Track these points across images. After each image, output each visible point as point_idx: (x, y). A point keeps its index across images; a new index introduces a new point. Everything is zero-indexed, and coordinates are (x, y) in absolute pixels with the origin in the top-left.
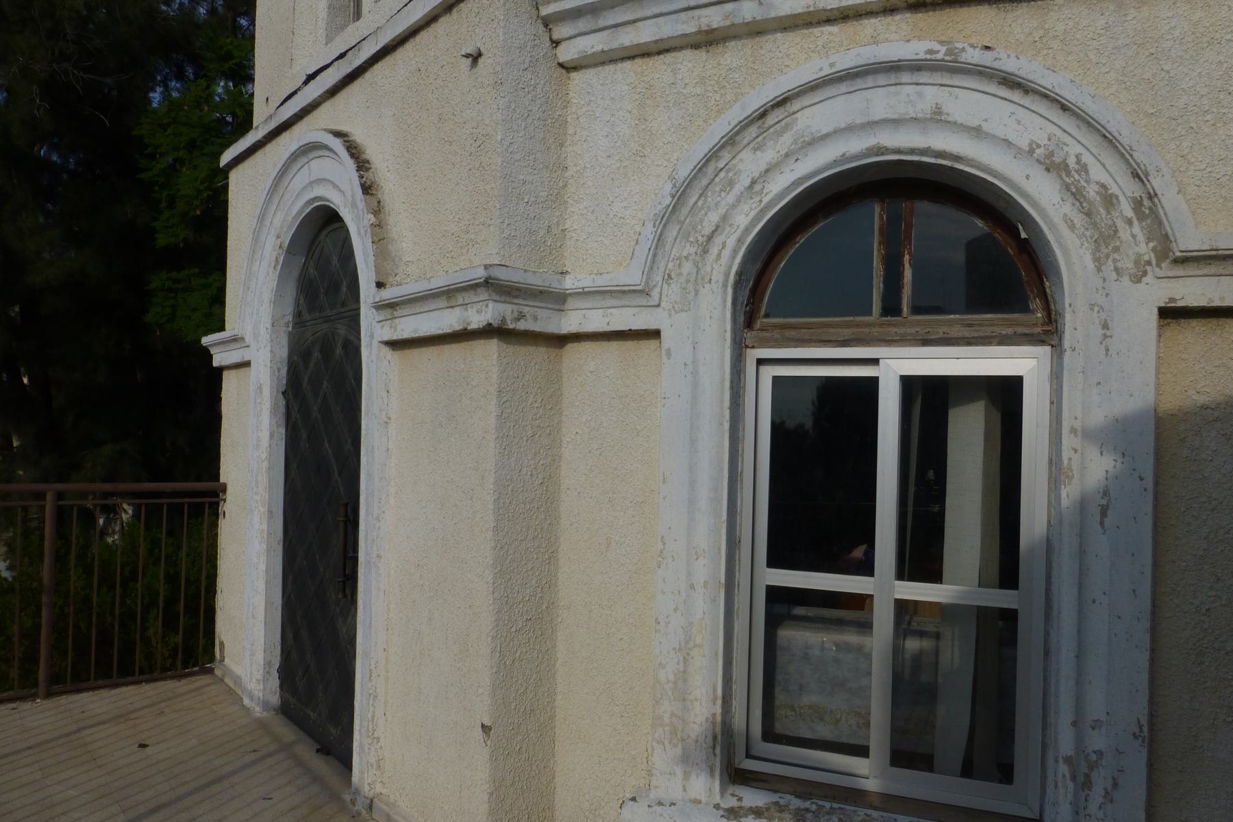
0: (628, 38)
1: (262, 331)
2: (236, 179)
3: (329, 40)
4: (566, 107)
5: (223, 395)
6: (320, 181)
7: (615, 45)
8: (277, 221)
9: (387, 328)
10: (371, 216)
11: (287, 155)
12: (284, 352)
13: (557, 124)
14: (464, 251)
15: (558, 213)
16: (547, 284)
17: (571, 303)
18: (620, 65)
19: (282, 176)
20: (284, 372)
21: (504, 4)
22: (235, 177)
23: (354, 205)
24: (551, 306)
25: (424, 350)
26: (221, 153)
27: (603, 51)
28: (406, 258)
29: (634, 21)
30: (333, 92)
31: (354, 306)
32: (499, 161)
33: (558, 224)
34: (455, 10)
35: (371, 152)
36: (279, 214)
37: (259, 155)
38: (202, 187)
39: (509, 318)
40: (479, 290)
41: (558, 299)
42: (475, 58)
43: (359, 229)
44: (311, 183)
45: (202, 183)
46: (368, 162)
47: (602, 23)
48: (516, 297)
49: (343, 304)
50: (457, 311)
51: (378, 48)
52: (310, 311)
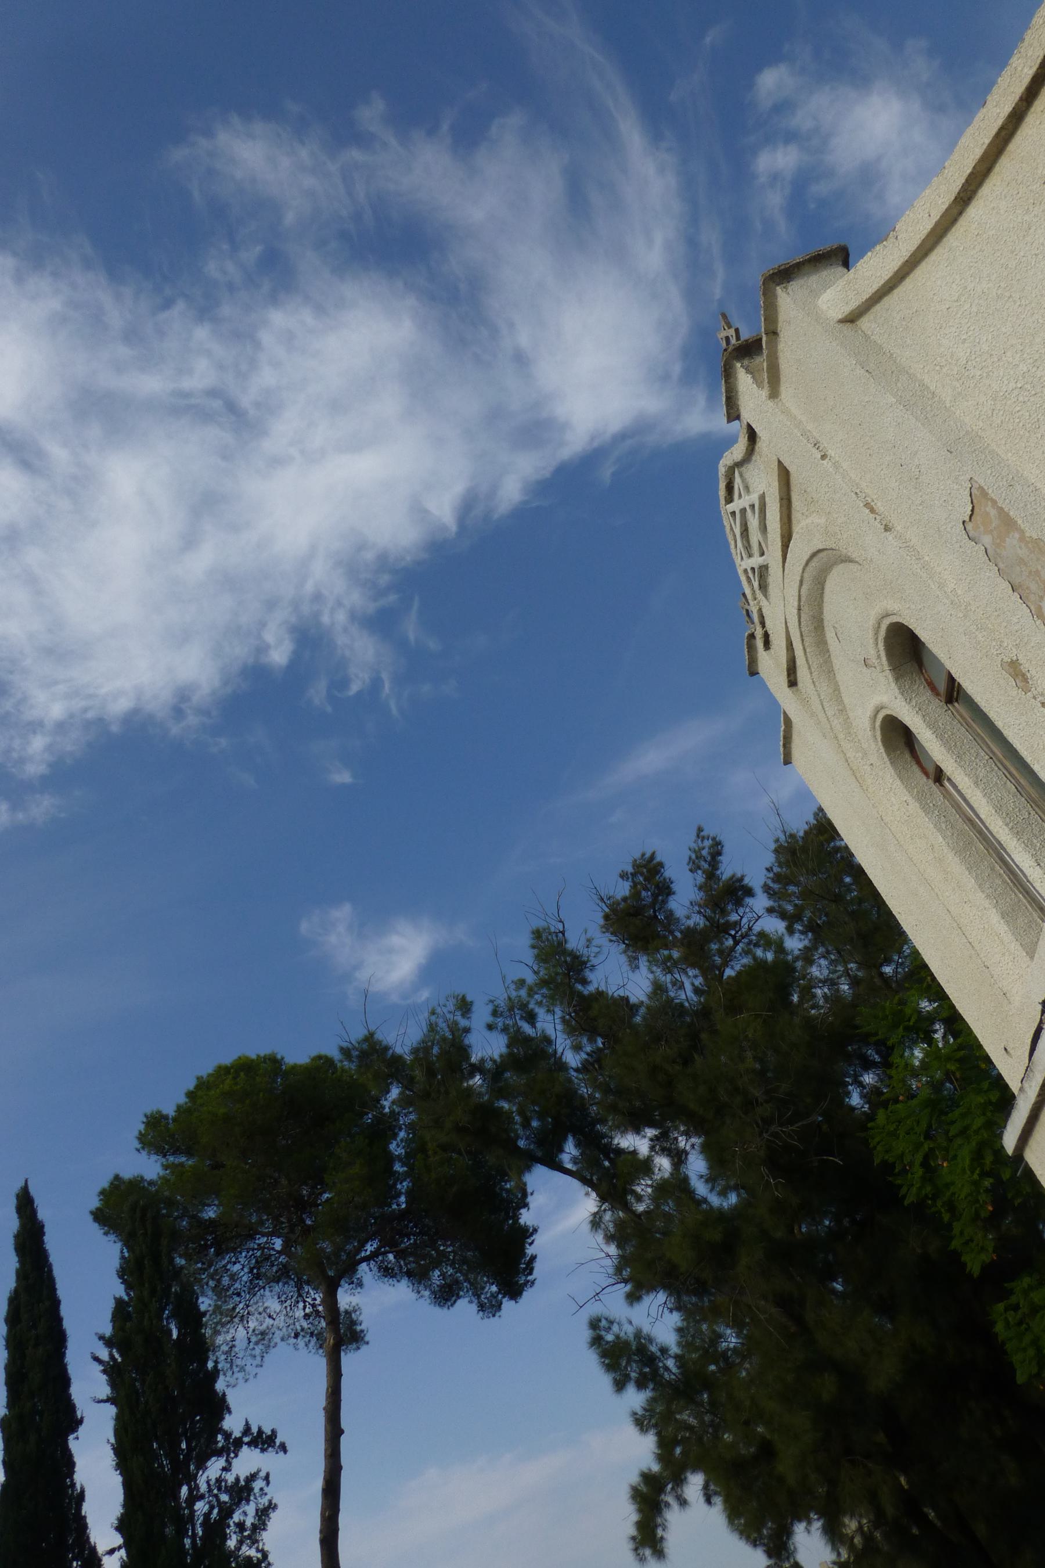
26: (1000, 1136)
45: (973, 1172)
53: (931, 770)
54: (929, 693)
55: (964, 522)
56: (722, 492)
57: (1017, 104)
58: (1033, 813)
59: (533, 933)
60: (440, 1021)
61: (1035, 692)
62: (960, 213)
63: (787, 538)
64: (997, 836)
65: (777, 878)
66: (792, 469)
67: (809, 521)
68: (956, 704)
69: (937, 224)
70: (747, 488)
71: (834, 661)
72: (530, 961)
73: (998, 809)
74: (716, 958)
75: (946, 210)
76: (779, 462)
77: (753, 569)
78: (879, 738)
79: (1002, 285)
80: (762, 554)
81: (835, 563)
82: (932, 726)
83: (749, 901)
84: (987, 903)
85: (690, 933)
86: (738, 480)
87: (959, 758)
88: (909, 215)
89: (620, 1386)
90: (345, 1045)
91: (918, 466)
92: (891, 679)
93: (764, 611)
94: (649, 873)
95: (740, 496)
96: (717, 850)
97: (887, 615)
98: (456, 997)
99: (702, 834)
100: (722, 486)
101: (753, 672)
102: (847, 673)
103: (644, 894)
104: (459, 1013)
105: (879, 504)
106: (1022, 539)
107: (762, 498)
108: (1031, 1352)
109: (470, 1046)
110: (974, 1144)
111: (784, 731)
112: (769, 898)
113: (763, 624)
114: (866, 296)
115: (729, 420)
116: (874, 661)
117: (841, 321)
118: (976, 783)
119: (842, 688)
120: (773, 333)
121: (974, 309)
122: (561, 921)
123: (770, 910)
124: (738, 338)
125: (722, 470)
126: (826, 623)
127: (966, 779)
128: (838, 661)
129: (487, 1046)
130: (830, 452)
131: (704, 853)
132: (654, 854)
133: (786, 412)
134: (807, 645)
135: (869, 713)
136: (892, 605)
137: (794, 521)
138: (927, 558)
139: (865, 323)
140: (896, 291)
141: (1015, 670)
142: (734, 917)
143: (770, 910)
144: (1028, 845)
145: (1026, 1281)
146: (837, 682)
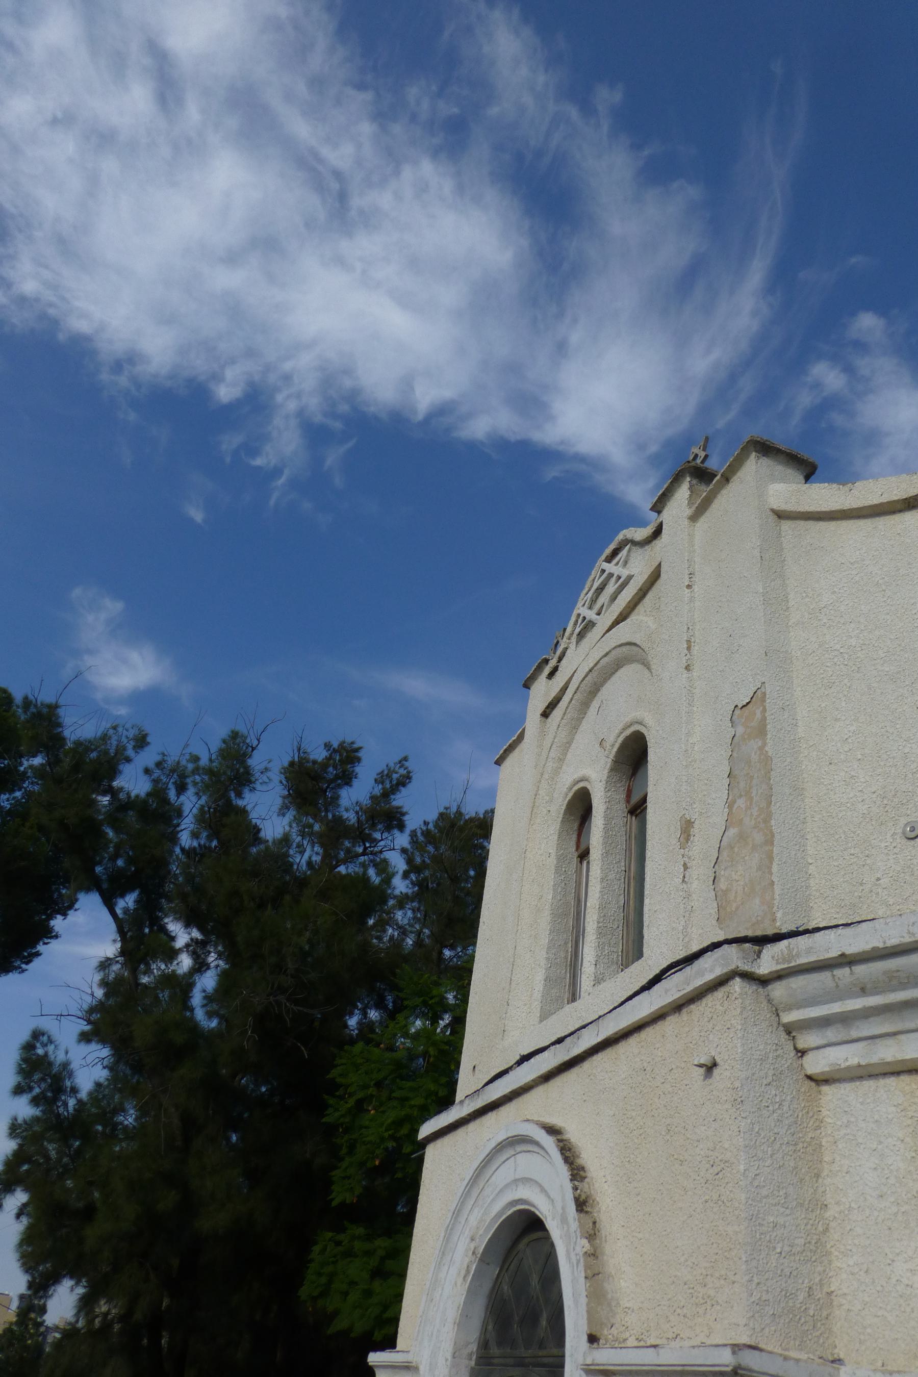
0: (888, 1052)
2: (433, 1155)
3: (544, 1017)
6: (526, 1180)
7: (874, 1059)
8: (474, 1219)
10: (585, 1242)
11: (493, 1144)
13: (810, 1149)
15: (820, 1269)
18: (882, 1082)
22: (431, 1152)
23: (564, 1220)
27: (859, 1066)
28: (625, 1303)
29: (895, 1034)
30: (547, 1077)
31: (555, 1351)
32: (743, 1197)
34: (684, 1011)
35: (588, 1157)
36: (476, 1211)
37: (460, 1132)
42: (710, 1068)
43: (568, 1251)
45: (386, 1130)
46: (583, 1169)
47: (854, 1034)
49: (541, 1346)
51: (599, 1039)
52: (500, 1344)
53: (583, 847)
54: (623, 796)
55: (736, 706)
56: (608, 551)
58: (621, 928)
59: (232, 732)
60: (115, 738)
61: (686, 853)
62: (900, 511)
64: (586, 925)
65: (427, 834)
66: (663, 575)
67: (645, 619)
68: (634, 818)
69: (881, 504)
70: (626, 563)
72: (214, 749)
73: (602, 908)
74: (342, 853)
77: (584, 618)
78: (569, 797)
79: (886, 579)
80: (599, 614)
81: (637, 661)
82: (608, 819)
83: (396, 832)
84: (543, 962)
85: (338, 820)
86: (624, 552)
87: (606, 854)
88: (870, 484)
89: (18, 1090)
90: (31, 697)
91: (740, 646)
93: (568, 651)
94: (346, 759)
95: (617, 564)
96: (405, 780)
97: (641, 723)
100: (612, 547)
101: (527, 685)
102: (585, 739)
103: (331, 769)
104: (132, 743)
105: (696, 648)
106: (761, 748)
107: (630, 578)
108: (323, 1280)
109: (120, 772)
110: (403, 1113)
112: (410, 843)
113: (560, 659)
115: (652, 509)
116: (608, 745)
117: (773, 510)
120: (726, 479)
121: (857, 578)
122: (258, 740)
123: (404, 851)
124: (703, 462)
125: (620, 537)
126: (599, 694)
127: (599, 871)
128: (585, 725)
129: (133, 782)
130: (696, 588)
131: (395, 776)
132: (361, 748)
133: (691, 536)
135: (576, 776)
136: (649, 720)
137: (636, 611)
138: (695, 709)
139: (786, 525)
140: (821, 524)
141: (687, 828)
142: (377, 835)
143: (404, 851)
144: (600, 947)
145: (360, 1231)
146: (573, 739)
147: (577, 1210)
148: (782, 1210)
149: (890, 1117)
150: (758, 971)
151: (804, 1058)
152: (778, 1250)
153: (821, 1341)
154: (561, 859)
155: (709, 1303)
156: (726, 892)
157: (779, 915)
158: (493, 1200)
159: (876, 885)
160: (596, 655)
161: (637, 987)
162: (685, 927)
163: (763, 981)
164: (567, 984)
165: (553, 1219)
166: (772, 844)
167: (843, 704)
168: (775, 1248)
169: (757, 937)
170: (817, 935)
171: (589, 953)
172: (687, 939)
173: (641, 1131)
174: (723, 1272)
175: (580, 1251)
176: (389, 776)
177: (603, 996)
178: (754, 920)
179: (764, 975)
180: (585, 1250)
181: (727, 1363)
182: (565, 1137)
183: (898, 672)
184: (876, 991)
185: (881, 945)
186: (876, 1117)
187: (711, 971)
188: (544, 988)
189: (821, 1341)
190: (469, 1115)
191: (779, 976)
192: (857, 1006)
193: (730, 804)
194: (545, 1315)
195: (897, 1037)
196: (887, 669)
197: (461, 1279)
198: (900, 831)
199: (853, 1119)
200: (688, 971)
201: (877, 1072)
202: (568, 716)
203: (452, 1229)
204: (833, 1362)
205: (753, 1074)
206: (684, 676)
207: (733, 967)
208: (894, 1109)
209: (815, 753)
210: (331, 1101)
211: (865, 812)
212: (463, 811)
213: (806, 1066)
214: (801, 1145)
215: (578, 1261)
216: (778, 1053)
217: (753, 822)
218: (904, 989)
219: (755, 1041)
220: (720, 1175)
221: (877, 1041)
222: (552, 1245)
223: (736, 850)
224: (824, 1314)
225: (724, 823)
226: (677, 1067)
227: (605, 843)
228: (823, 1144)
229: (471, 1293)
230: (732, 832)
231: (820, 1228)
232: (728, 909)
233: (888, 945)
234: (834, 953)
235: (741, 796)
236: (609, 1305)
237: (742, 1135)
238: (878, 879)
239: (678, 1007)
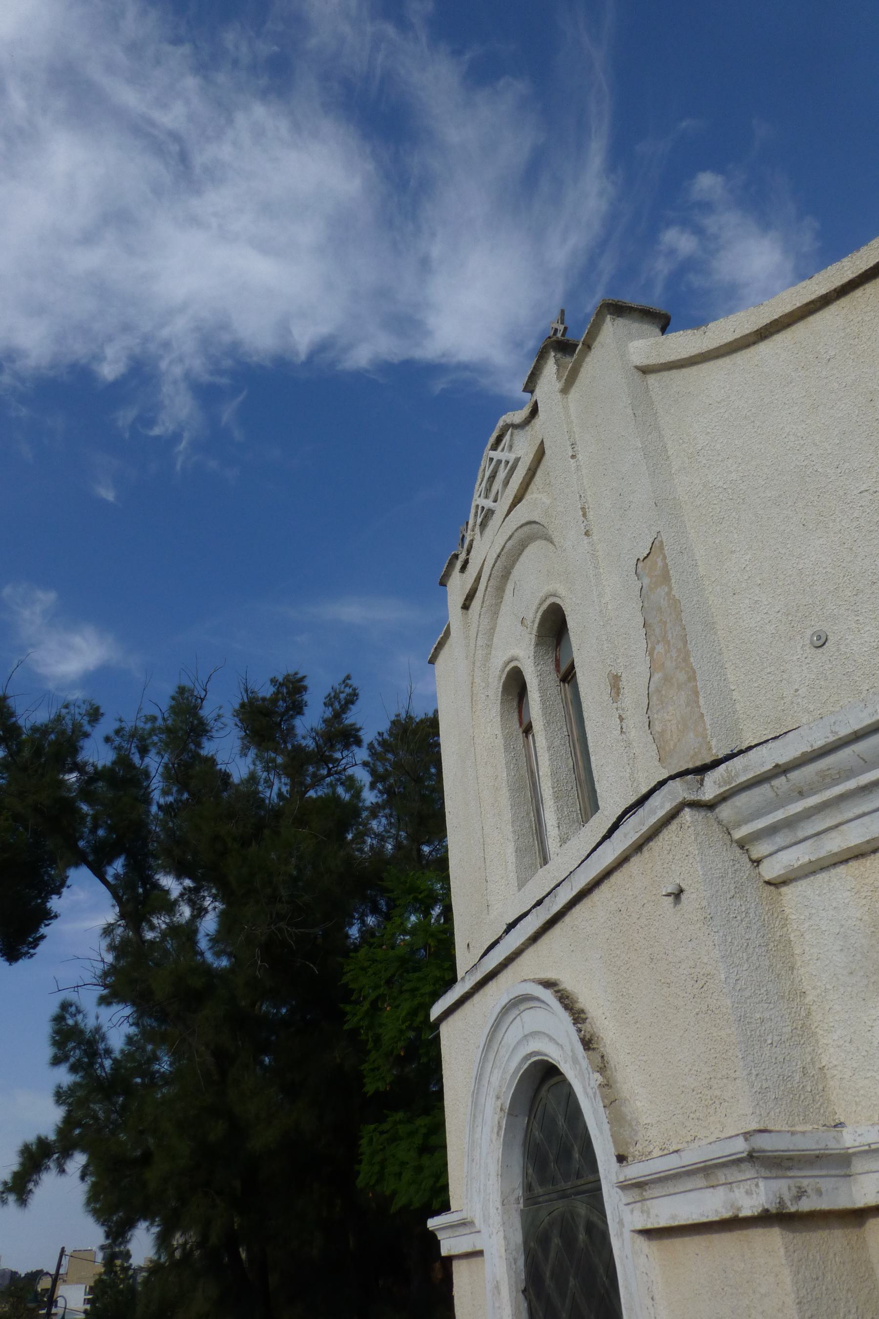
0: (835, 844)
1: (493, 1211)
3: (522, 884)
4: (785, 925)
5: (456, 1292)
6: (534, 1034)
7: (823, 853)
8: (496, 1079)
9: (637, 1213)
10: (597, 1075)
12: (518, 1238)
13: (780, 947)
14: (712, 1111)
15: (809, 1049)
16: (822, 1146)
17: (858, 1166)
18: (833, 872)
19: (495, 1031)
20: (521, 1262)
21: (696, 839)
22: (446, 1031)
23: (575, 1061)
24: (833, 1172)
25: (687, 1239)
27: (811, 862)
28: (644, 1120)
29: (837, 826)
30: (535, 938)
31: (591, 1178)
32: (729, 1002)
33: (813, 1062)
34: (645, 849)
35: (585, 1000)
36: (496, 1071)
38: (404, 1027)
39: (787, 1198)
40: (743, 1166)
41: (841, 1162)
42: (677, 895)
43: (584, 1088)
44: (525, 1036)
45: (403, 1023)
46: (582, 1011)
47: (801, 835)
48: (790, 1168)
49: (579, 1176)
50: (721, 1192)
51: (574, 893)
52: (542, 1184)
53: (525, 723)
54: (553, 667)
57: (830, 292)
58: (575, 788)
59: (179, 688)
60: (68, 717)
61: (619, 705)
62: (754, 343)
63: (518, 499)
65: (383, 743)
67: (539, 496)
69: (736, 340)
70: (511, 447)
71: (503, 607)
73: (554, 774)
74: (308, 779)
75: (747, 335)
76: (542, 442)
77: (483, 508)
79: (753, 410)
80: (495, 501)
81: (540, 538)
82: (542, 691)
83: (355, 748)
84: (511, 836)
86: (507, 438)
87: (548, 723)
88: (721, 323)
91: (631, 502)
92: (533, 642)
93: (475, 543)
94: (293, 690)
95: (503, 450)
96: (352, 698)
97: (555, 595)
98: (91, 705)
99: (348, 681)
100: (495, 435)
101: (443, 583)
102: (507, 621)
103: (281, 703)
105: (592, 513)
106: (669, 593)
107: (517, 460)
109: (82, 748)
110: (416, 1002)
111: (442, 638)
112: (370, 756)
113: (468, 552)
114: (663, 361)
115: (525, 390)
116: (528, 622)
117: (637, 368)
118: (549, 747)
119: (497, 629)
120: (588, 346)
121: (726, 416)
122: (205, 690)
123: (365, 764)
124: (563, 335)
125: (501, 423)
126: (511, 577)
127: (544, 741)
128: (504, 608)
129: (97, 754)
130: (580, 457)
131: (342, 696)
132: (304, 677)
133: (566, 408)
134: (490, 584)
135: (505, 658)
136: (562, 590)
137: (529, 490)
138: (601, 570)
139: (652, 379)
140: (684, 370)
141: (615, 682)
142: (338, 755)
143: (365, 764)
144: (559, 810)
145: (400, 1115)
147: (585, 1050)
148: (766, 1005)
149: (846, 901)
150: (703, 799)
151: (760, 866)
152: (769, 1042)
153: (822, 1111)
154: (507, 738)
155: (717, 1102)
156: (662, 733)
157: (713, 743)
158: (508, 1060)
159: (796, 696)
160: (500, 540)
161: (599, 839)
162: (632, 774)
163: (710, 806)
164: (536, 849)
165: (566, 1062)
166: (695, 679)
167: (736, 536)
168: (766, 1041)
169: (697, 767)
170: (751, 753)
171: (550, 817)
172: (635, 784)
173: (628, 966)
174: (724, 1073)
175: (594, 1084)
176: (336, 697)
177: (571, 854)
178: (692, 752)
179: (709, 801)
180: (598, 1082)
181: (741, 1149)
182: (561, 988)
183: (780, 496)
184: (813, 791)
185: (809, 749)
186: (834, 904)
187: (662, 807)
188: (516, 859)
189: (822, 1111)
190: (472, 988)
191: (723, 798)
192: (799, 809)
193: (650, 652)
194: (576, 1149)
195: (841, 828)
196: (769, 495)
197: (495, 1135)
198: (808, 642)
199: (814, 911)
200: (641, 812)
201: (826, 864)
202: (487, 603)
203: (477, 1093)
204: (835, 1126)
205: (717, 891)
206: (585, 542)
207: (680, 799)
208: (848, 893)
209: (718, 587)
210: (348, 1008)
211: (774, 631)
212: (412, 715)
213: (763, 873)
214: (772, 944)
215: (595, 1094)
216: (736, 867)
217: (674, 663)
218: (837, 784)
219: (713, 862)
220: (705, 988)
221: (822, 836)
222: (570, 1085)
223: (664, 692)
224: (820, 1087)
225: (648, 670)
226: (648, 901)
227: (544, 714)
228: (792, 939)
229: (507, 1145)
230: (657, 677)
231: (803, 1014)
232: (667, 749)
233: (815, 747)
234: (769, 766)
235: (658, 642)
236: (630, 1125)
237: (717, 947)
238: (797, 690)
239: (638, 847)
